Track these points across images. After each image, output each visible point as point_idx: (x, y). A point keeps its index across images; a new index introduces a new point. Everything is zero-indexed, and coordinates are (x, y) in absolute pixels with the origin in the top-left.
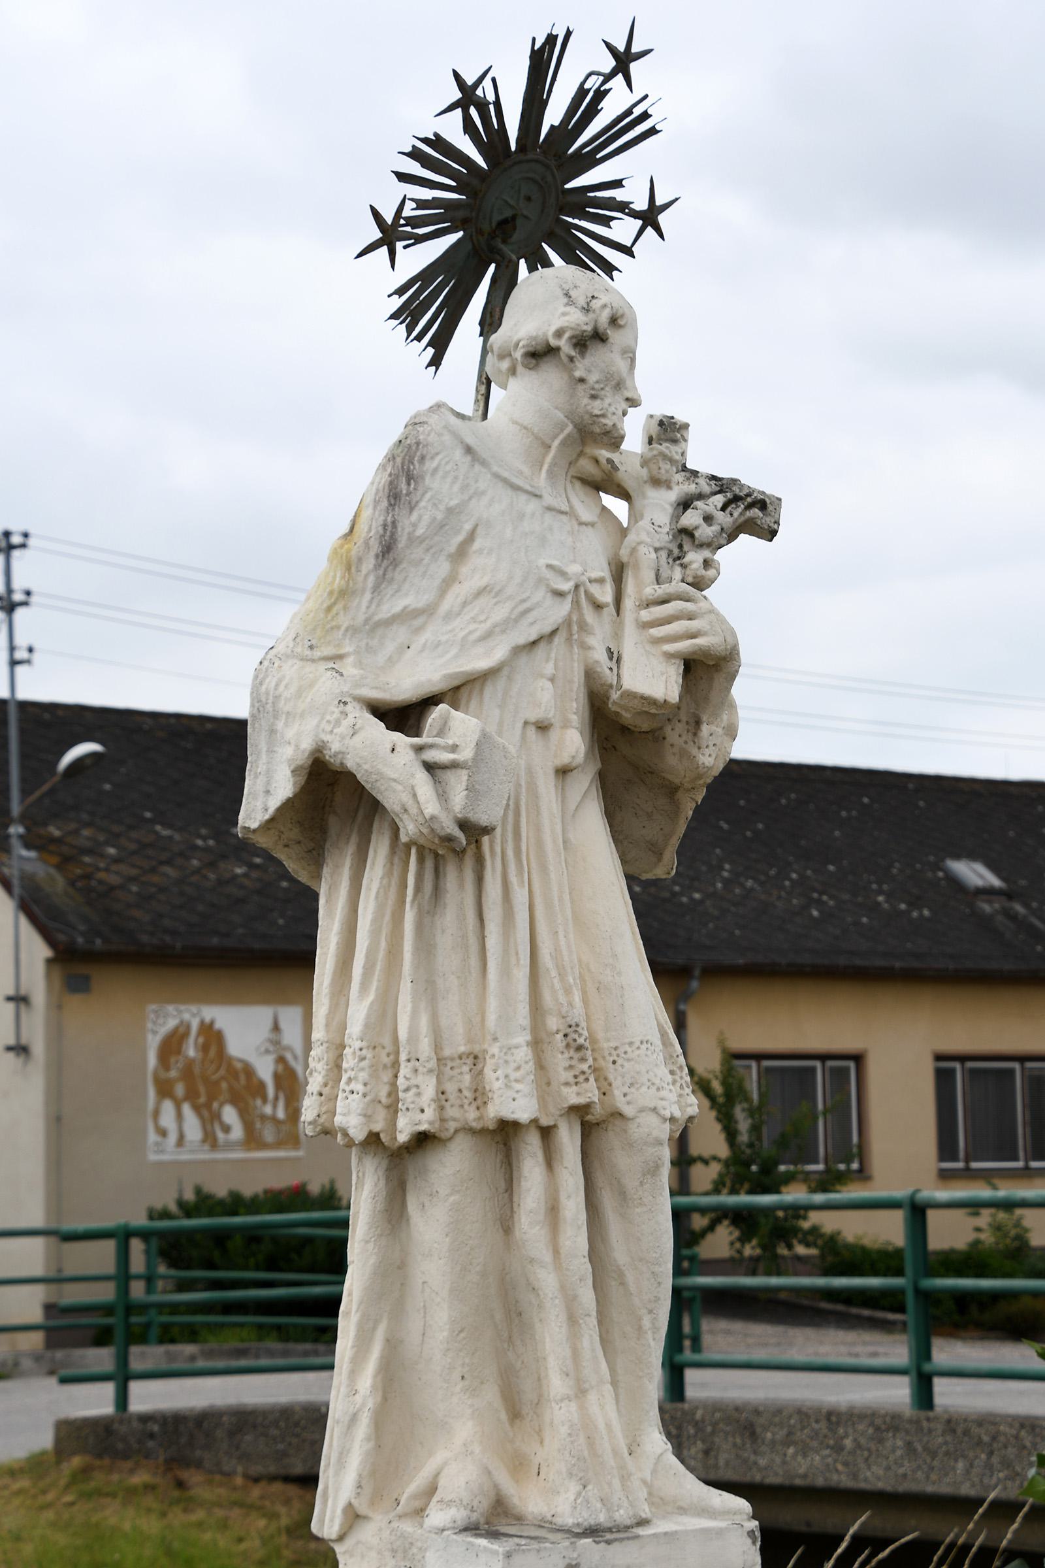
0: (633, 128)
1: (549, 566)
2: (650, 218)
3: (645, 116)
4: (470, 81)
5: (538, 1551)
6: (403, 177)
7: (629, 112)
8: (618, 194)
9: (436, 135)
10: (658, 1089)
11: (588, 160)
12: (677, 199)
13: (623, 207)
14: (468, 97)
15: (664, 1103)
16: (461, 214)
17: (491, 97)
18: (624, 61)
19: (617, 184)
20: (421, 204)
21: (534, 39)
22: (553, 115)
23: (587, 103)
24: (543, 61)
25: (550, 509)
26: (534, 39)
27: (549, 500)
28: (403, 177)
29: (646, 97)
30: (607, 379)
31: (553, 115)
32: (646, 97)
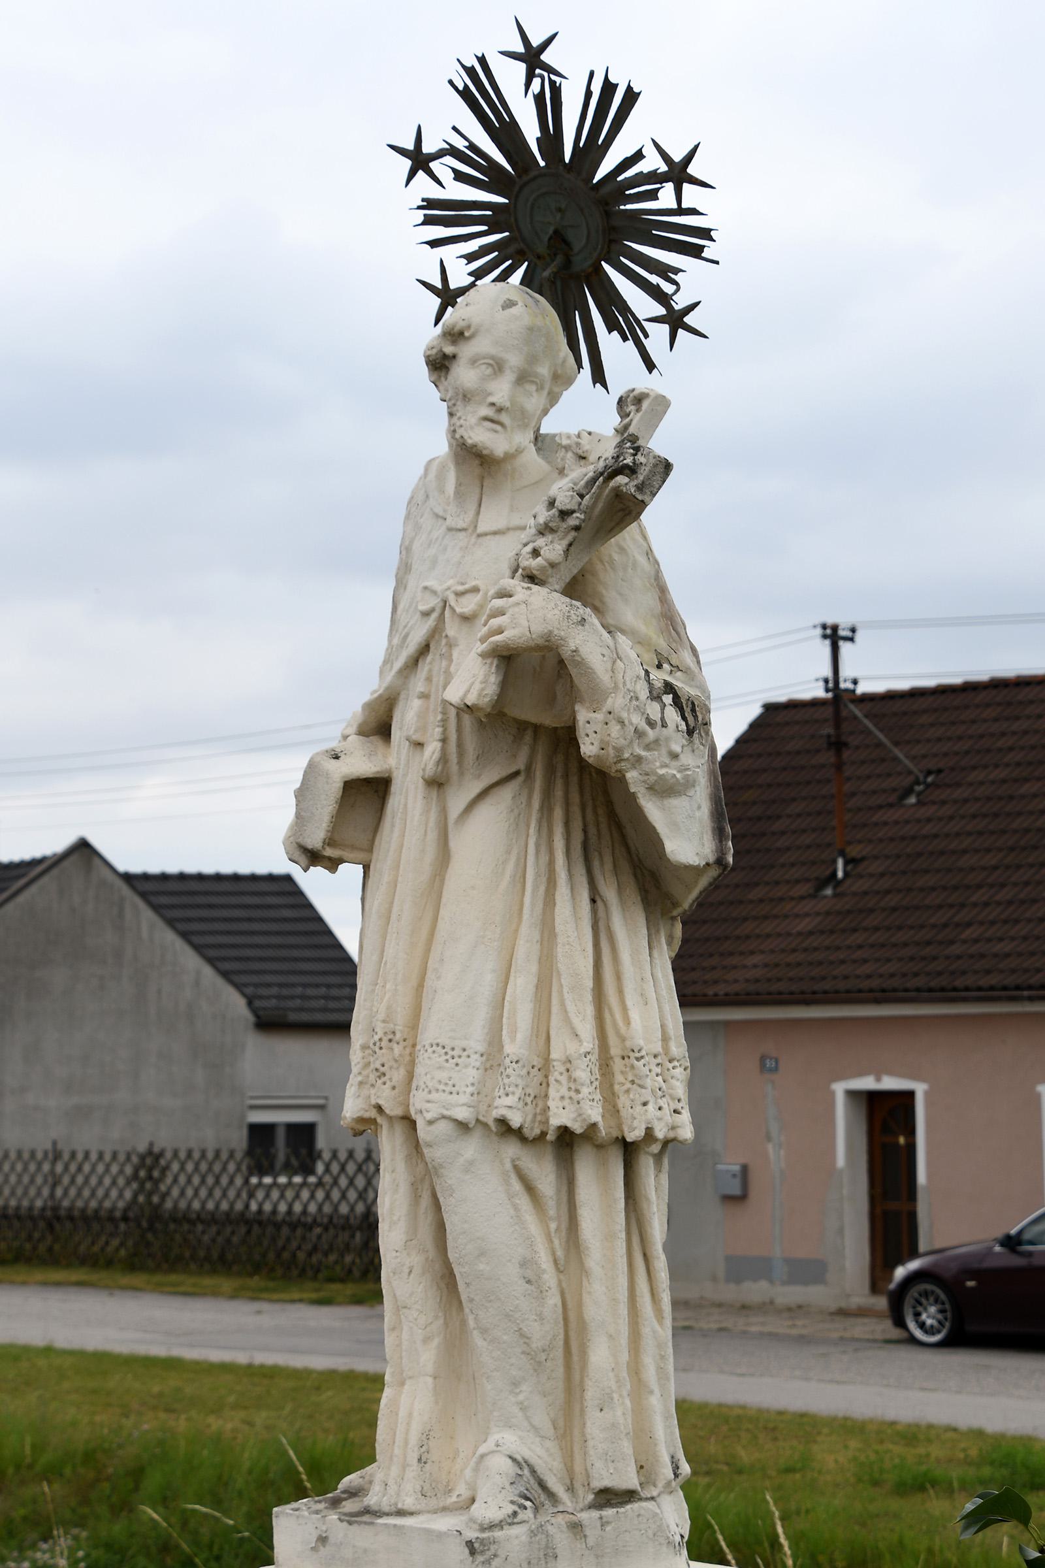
0: (613, 104)
1: (426, 588)
2: (678, 173)
3: (609, 88)
4: (410, 146)
5: (298, 1517)
6: (434, 244)
7: (588, 94)
8: (643, 167)
9: (423, 200)
10: (430, 1092)
11: (591, 150)
12: (696, 147)
13: (654, 177)
14: (419, 161)
15: (429, 1105)
16: (511, 250)
17: (460, 144)
18: (532, 58)
19: (638, 156)
20: (470, 258)
21: (451, 82)
22: (531, 131)
23: (549, 105)
24: (478, 90)
25: (450, 529)
26: (451, 82)
27: (450, 522)
28: (434, 244)
29: (592, 74)
30: (457, 394)
31: (531, 131)
32: (592, 74)
